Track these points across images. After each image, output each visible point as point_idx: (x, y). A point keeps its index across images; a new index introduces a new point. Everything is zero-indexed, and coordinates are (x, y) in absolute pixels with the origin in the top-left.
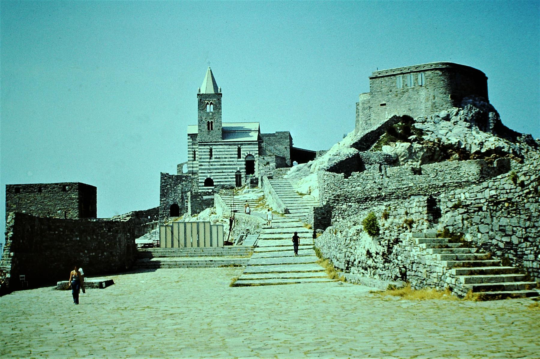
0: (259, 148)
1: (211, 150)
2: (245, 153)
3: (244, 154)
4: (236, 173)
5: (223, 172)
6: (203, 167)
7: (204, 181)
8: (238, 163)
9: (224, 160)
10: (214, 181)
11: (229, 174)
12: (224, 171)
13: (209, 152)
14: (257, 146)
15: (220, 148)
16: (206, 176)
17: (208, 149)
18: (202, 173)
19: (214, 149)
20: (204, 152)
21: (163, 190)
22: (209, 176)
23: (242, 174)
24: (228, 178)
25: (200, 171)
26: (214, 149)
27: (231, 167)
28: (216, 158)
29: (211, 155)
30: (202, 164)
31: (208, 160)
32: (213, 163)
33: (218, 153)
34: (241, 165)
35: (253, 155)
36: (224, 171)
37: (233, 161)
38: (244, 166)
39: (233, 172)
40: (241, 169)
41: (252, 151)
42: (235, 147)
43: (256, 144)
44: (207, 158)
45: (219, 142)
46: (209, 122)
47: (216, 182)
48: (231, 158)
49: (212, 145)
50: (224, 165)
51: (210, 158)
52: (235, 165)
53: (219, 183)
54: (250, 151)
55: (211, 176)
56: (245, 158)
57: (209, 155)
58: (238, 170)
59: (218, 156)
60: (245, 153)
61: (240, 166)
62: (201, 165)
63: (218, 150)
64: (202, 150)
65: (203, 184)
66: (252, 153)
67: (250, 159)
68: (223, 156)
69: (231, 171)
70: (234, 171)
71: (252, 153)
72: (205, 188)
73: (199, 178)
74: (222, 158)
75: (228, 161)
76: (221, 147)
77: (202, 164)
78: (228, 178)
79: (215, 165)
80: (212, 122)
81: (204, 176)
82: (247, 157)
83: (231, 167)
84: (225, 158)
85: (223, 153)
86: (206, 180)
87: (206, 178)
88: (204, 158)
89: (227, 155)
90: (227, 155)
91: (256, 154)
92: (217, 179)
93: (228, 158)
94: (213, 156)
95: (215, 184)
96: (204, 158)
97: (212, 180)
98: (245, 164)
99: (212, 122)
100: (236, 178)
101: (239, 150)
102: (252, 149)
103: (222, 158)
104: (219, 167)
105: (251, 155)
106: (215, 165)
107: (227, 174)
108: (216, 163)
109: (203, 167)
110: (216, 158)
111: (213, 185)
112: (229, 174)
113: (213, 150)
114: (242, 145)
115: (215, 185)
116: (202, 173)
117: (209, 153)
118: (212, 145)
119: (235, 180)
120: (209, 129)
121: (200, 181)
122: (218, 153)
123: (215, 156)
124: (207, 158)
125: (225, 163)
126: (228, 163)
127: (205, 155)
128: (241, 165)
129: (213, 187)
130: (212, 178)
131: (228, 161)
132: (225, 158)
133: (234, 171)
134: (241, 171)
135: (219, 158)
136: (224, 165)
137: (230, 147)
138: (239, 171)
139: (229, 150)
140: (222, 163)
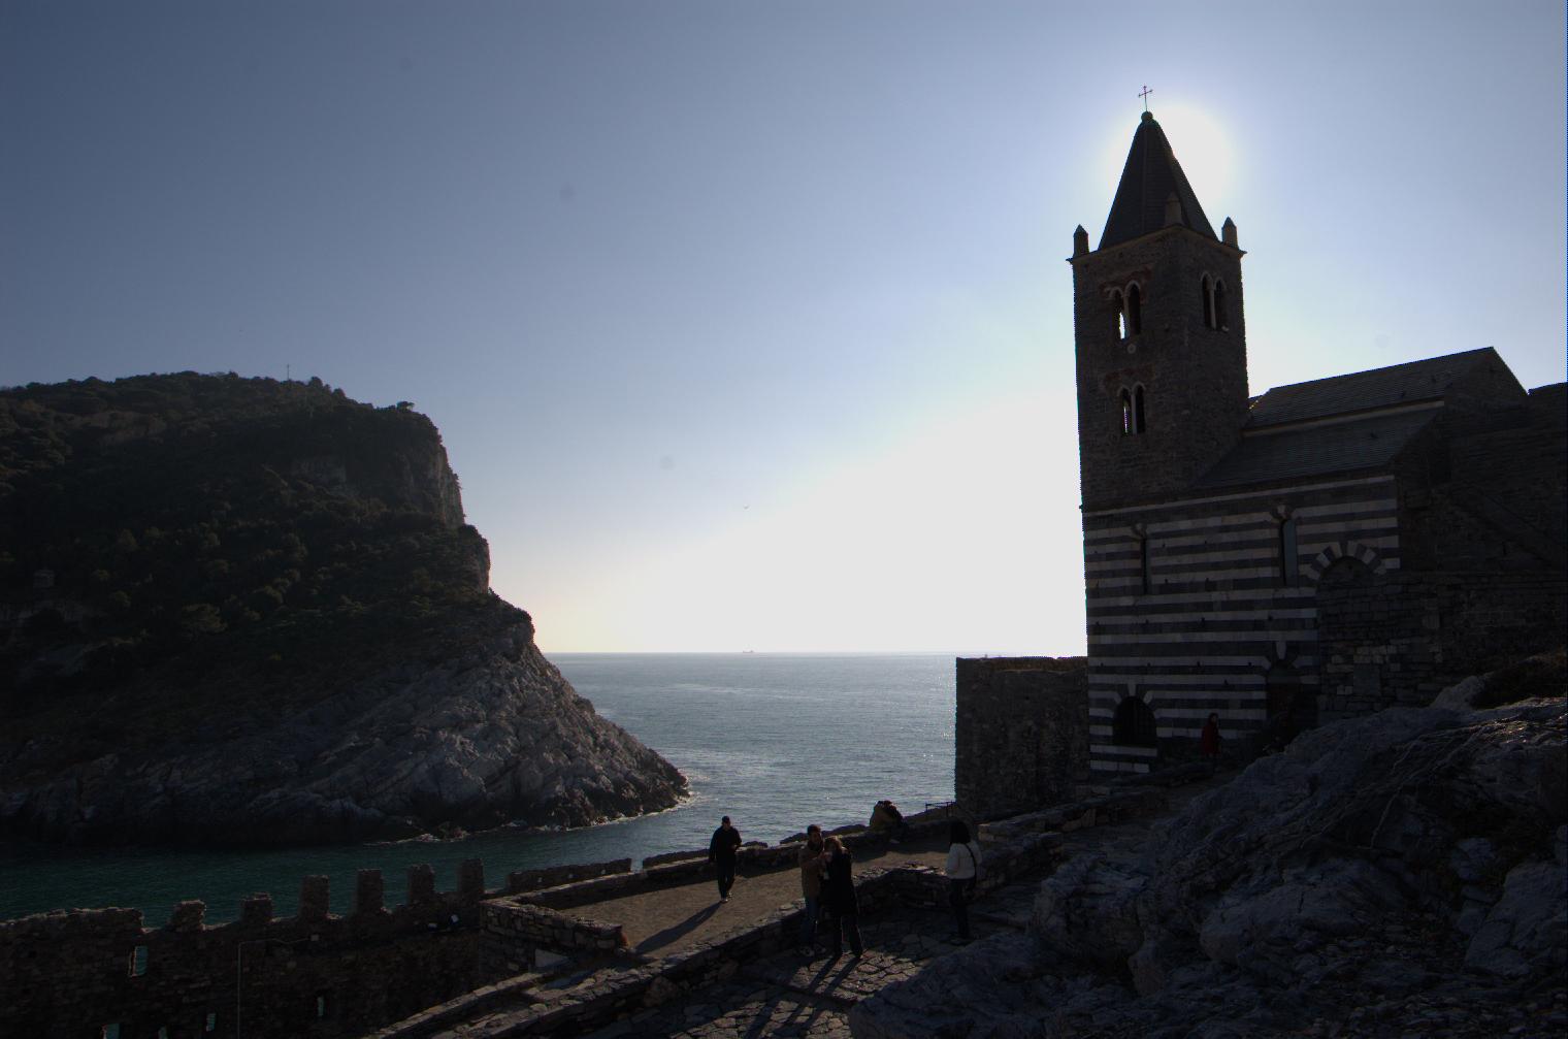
2: (1317, 548)
3: (1309, 559)
5: (1198, 669)
7: (1111, 714)
11: (1233, 679)
12: (1207, 661)
14: (1392, 504)
16: (1122, 688)
17: (1123, 539)
19: (1157, 536)
22: (1132, 682)
27: (1243, 636)
28: (1166, 589)
29: (1143, 572)
31: (1127, 601)
33: (1173, 561)
34: (1290, 625)
35: (1368, 558)
36: (1207, 661)
37: (1249, 605)
39: (1248, 669)
40: (1294, 648)
41: (1357, 534)
42: (1258, 517)
44: (1122, 591)
47: (1167, 722)
48: (1239, 584)
49: (1145, 517)
50: (1204, 626)
52: (1258, 625)
55: (1142, 689)
59: (1173, 579)
60: (1317, 548)
61: (1295, 636)
63: (1171, 542)
65: (1109, 731)
66: (1362, 549)
68: (1201, 577)
69: (1240, 661)
70: (1255, 660)
71: (1362, 549)
72: (1112, 750)
73: (1093, 694)
74: (1193, 587)
75: (1227, 606)
76: (1185, 524)
79: (1159, 628)
80: (1140, 389)
81: (1111, 687)
82: (1326, 572)
83: (1243, 636)
84: (1210, 586)
85: (1201, 558)
89: (1216, 566)
90: (1216, 566)
91: (1387, 553)
92: (1172, 704)
99: (1140, 389)
102: (1355, 525)
104: (1178, 638)
106: (1159, 628)
107: (1218, 679)
108: (1163, 618)
110: (1166, 589)
111: (1151, 741)
112: (1233, 679)
113: (1154, 544)
114: (1297, 501)
118: (1145, 517)
121: (1093, 712)
122: (1173, 561)
124: (1122, 591)
125: (1209, 616)
128: (1290, 625)
129: (1152, 753)
131: (1227, 606)
132: (1210, 586)
133: (1255, 660)
135: (1179, 588)
136: (1204, 626)
137: (1233, 520)
139: (1226, 538)
140: (1196, 617)
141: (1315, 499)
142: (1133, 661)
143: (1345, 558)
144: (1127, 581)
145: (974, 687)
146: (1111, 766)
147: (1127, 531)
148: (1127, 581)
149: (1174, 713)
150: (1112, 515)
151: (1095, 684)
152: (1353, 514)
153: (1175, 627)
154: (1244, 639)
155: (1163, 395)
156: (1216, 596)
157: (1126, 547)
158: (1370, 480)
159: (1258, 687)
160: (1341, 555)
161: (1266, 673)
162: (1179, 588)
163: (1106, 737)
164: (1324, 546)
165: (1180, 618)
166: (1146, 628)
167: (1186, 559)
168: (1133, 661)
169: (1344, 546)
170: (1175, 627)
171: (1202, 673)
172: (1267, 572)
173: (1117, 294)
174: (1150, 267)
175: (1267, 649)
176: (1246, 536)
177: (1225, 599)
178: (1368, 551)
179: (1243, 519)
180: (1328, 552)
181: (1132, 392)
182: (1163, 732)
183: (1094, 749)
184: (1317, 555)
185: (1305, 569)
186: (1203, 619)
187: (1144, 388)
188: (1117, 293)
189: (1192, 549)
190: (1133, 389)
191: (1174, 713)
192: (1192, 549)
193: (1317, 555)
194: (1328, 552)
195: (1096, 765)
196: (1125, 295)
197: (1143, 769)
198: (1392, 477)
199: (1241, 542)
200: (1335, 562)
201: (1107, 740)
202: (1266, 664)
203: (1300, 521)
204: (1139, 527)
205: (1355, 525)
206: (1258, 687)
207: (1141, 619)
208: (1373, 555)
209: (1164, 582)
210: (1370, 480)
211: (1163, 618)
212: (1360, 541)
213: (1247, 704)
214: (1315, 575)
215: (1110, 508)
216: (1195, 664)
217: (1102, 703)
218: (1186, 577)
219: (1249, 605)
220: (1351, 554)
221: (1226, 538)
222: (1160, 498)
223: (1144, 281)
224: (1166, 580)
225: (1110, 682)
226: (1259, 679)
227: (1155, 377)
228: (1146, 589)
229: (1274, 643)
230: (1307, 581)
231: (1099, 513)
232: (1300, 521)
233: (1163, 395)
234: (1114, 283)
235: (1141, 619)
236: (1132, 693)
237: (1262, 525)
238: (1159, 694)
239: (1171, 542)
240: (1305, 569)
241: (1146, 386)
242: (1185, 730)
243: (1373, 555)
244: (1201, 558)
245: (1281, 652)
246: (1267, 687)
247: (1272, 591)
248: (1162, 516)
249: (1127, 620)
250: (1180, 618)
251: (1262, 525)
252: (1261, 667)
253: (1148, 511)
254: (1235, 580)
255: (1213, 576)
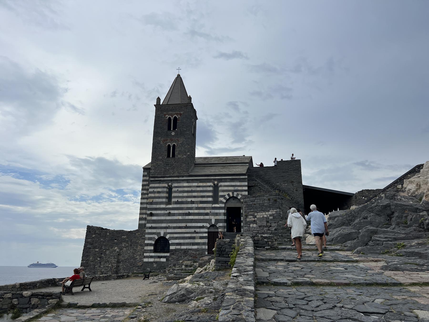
0: (249, 187)
1: (170, 189)
3: (223, 196)
4: (208, 228)
5: (186, 227)
6: (154, 218)
7: (153, 242)
8: (213, 211)
9: (190, 206)
10: (170, 242)
11: (198, 230)
13: (167, 192)
14: (246, 184)
15: (184, 187)
16: (159, 234)
17: (164, 187)
18: (151, 228)
19: (176, 187)
20: (159, 192)
21: (88, 256)
22: (162, 232)
23: (220, 230)
24: (194, 238)
25: (148, 225)
26: (176, 187)
27: (202, 217)
28: (177, 203)
29: (169, 198)
30: (154, 212)
32: (172, 212)
33: (181, 195)
34: (217, 214)
35: (239, 197)
37: (204, 208)
38: (223, 217)
39: (203, 227)
40: (217, 221)
42: (209, 184)
43: (245, 179)
45: (183, 177)
46: (169, 146)
50: (189, 214)
51: (169, 202)
52: (207, 214)
53: (178, 247)
54: (233, 191)
55: (166, 234)
56: (225, 203)
57: (167, 198)
58: (213, 223)
59: (180, 200)
60: (226, 193)
62: (151, 215)
63: (180, 189)
64: (156, 190)
65: (152, 248)
66: (238, 195)
67: (233, 204)
68: (189, 200)
70: (205, 224)
71: (238, 195)
73: (147, 236)
74: (187, 203)
76: (186, 184)
77: (154, 212)
78: (194, 238)
79: (174, 215)
80: (174, 145)
82: (227, 200)
83: (202, 217)
84: (192, 202)
85: (190, 194)
86: (157, 241)
87: (156, 237)
88: (157, 203)
89: (195, 197)
90: (195, 197)
93: (197, 202)
94: (174, 200)
95: (172, 248)
96: (157, 203)
97: (167, 241)
98: (224, 214)
99: (174, 145)
100: (208, 238)
101: (216, 188)
102: (236, 188)
103: (187, 203)
104: (180, 218)
105: (236, 198)
106: (174, 215)
108: (176, 212)
109: (154, 218)
110: (177, 203)
111: (168, 251)
112: (198, 230)
113: (174, 190)
115: (172, 250)
116: (151, 228)
117: (167, 195)
118: (171, 180)
119: (206, 241)
120: (169, 156)
121: (146, 242)
122: (181, 195)
123: (176, 200)
125: (191, 211)
126: (196, 211)
127: (159, 198)
128: (217, 214)
129: (168, 254)
130: (167, 237)
132: (192, 202)
133: (205, 224)
134: (218, 226)
135: (182, 203)
136: (189, 214)
137: (201, 184)
138: (212, 226)
139: (198, 189)
140: (187, 211)
141: (225, 180)
142: (164, 225)
143: (233, 197)
144: (164, 200)
145: (94, 236)
146: (152, 260)
147: (166, 185)
148: (164, 200)
149: (177, 241)
150: (161, 180)
151: (148, 233)
152: (236, 185)
153: (180, 214)
154: (202, 218)
155: (182, 148)
156: (194, 205)
157: (165, 190)
158: (241, 177)
159: (205, 233)
160: (232, 196)
161: (208, 228)
162: (182, 203)
163: (150, 250)
164: (228, 193)
165: (181, 212)
166: (169, 214)
167: (185, 194)
168: (164, 225)
169: (233, 194)
170: (180, 214)
171: (187, 228)
172: (210, 199)
173: (170, 118)
174: (182, 113)
175: (209, 221)
176: (205, 189)
177: (197, 206)
178: (240, 195)
179: (204, 184)
180: (229, 195)
181: (171, 145)
182: (172, 248)
183: (145, 254)
184: (226, 195)
185: (221, 199)
186: (189, 212)
187: (176, 145)
188: (170, 118)
189: (188, 192)
190: (172, 145)
191: (177, 241)
192: (188, 192)
193: (226, 195)
194: (229, 195)
195: (146, 260)
196: (172, 118)
197: (164, 260)
198: (247, 177)
199: (203, 190)
200: (230, 198)
201: (150, 251)
202: (208, 225)
203: (221, 186)
204: (170, 184)
205: (236, 188)
206: (205, 233)
207: (167, 212)
208: (241, 196)
209: (177, 201)
210: (241, 177)
211: (176, 212)
212: (237, 192)
213: (201, 238)
214: (225, 201)
215: (161, 177)
216: (185, 226)
217: (150, 239)
218: (184, 200)
219: (204, 208)
220: (235, 196)
221: (198, 189)
222: (178, 177)
223: (179, 116)
224: (178, 200)
225: (154, 232)
226: (206, 230)
227: (180, 143)
228: (169, 202)
229: (211, 219)
230: (222, 202)
231: (156, 179)
232: (221, 186)
233: (182, 148)
234: (169, 115)
235: (167, 212)
236: (162, 235)
237: (209, 186)
238: (172, 235)
239: (180, 189)
240: (221, 199)
241: (177, 145)
242: (180, 246)
243: (241, 196)
244: (190, 194)
245: (213, 223)
246: (208, 233)
247: (211, 204)
248: (177, 181)
249: (163, 212)
250: (181, 212)
251: (209, 186)
252: (207, 226)
253: (173, 180)
254: (200, 201)
255: (193, 199)
